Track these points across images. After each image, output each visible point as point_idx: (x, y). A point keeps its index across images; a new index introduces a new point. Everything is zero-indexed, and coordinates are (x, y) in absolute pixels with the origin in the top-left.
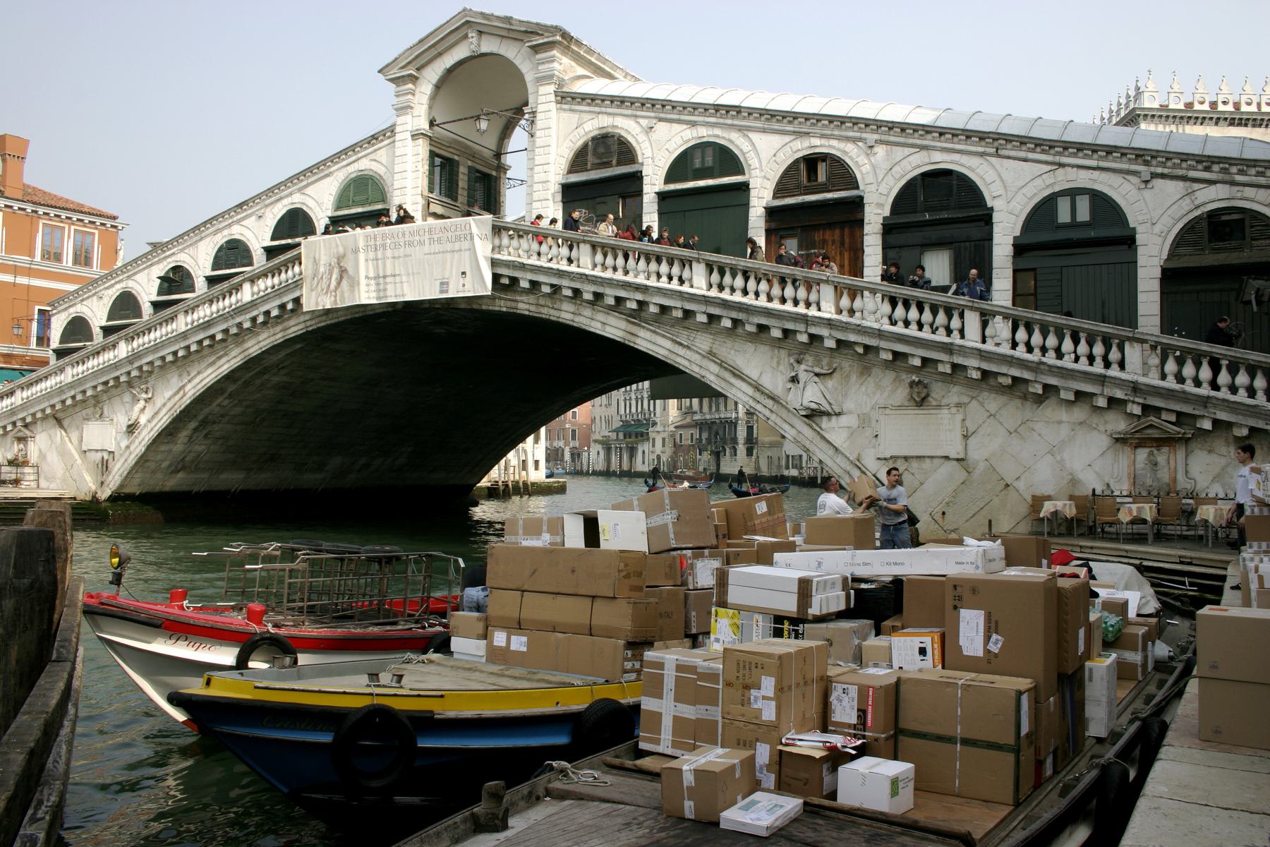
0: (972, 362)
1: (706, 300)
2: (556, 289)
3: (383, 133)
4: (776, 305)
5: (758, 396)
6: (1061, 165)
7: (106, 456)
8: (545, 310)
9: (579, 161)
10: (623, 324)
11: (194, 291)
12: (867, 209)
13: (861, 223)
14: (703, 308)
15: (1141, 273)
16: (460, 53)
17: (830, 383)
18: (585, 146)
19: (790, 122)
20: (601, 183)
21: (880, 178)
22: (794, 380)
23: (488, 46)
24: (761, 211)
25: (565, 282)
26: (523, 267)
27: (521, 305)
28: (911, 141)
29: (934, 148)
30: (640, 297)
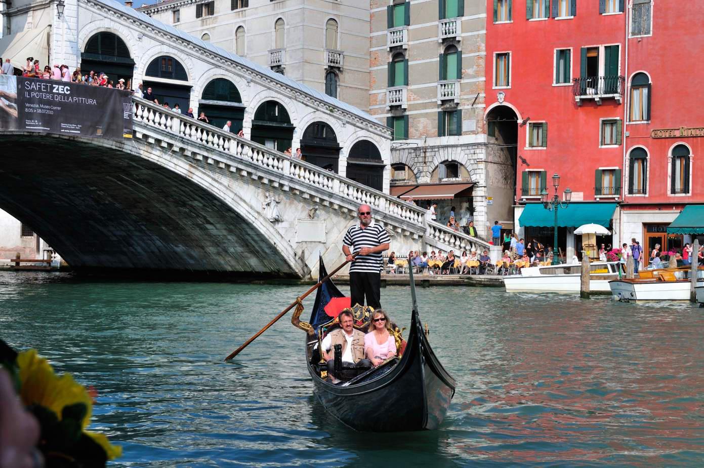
2: (158, 141)
5: (250, 210)
6: (318, 110)
8: (142, 152)
10: (187, 167)
12: (245, 115)
14: (235, 164)
17: (279, 205)
19: (213, 58)
21: (252, 98)
22: (268, 205)
25: (167, 140)
27: (126, 147)
28: (264, 84)
29: (273, 90)
30: (206, 154)
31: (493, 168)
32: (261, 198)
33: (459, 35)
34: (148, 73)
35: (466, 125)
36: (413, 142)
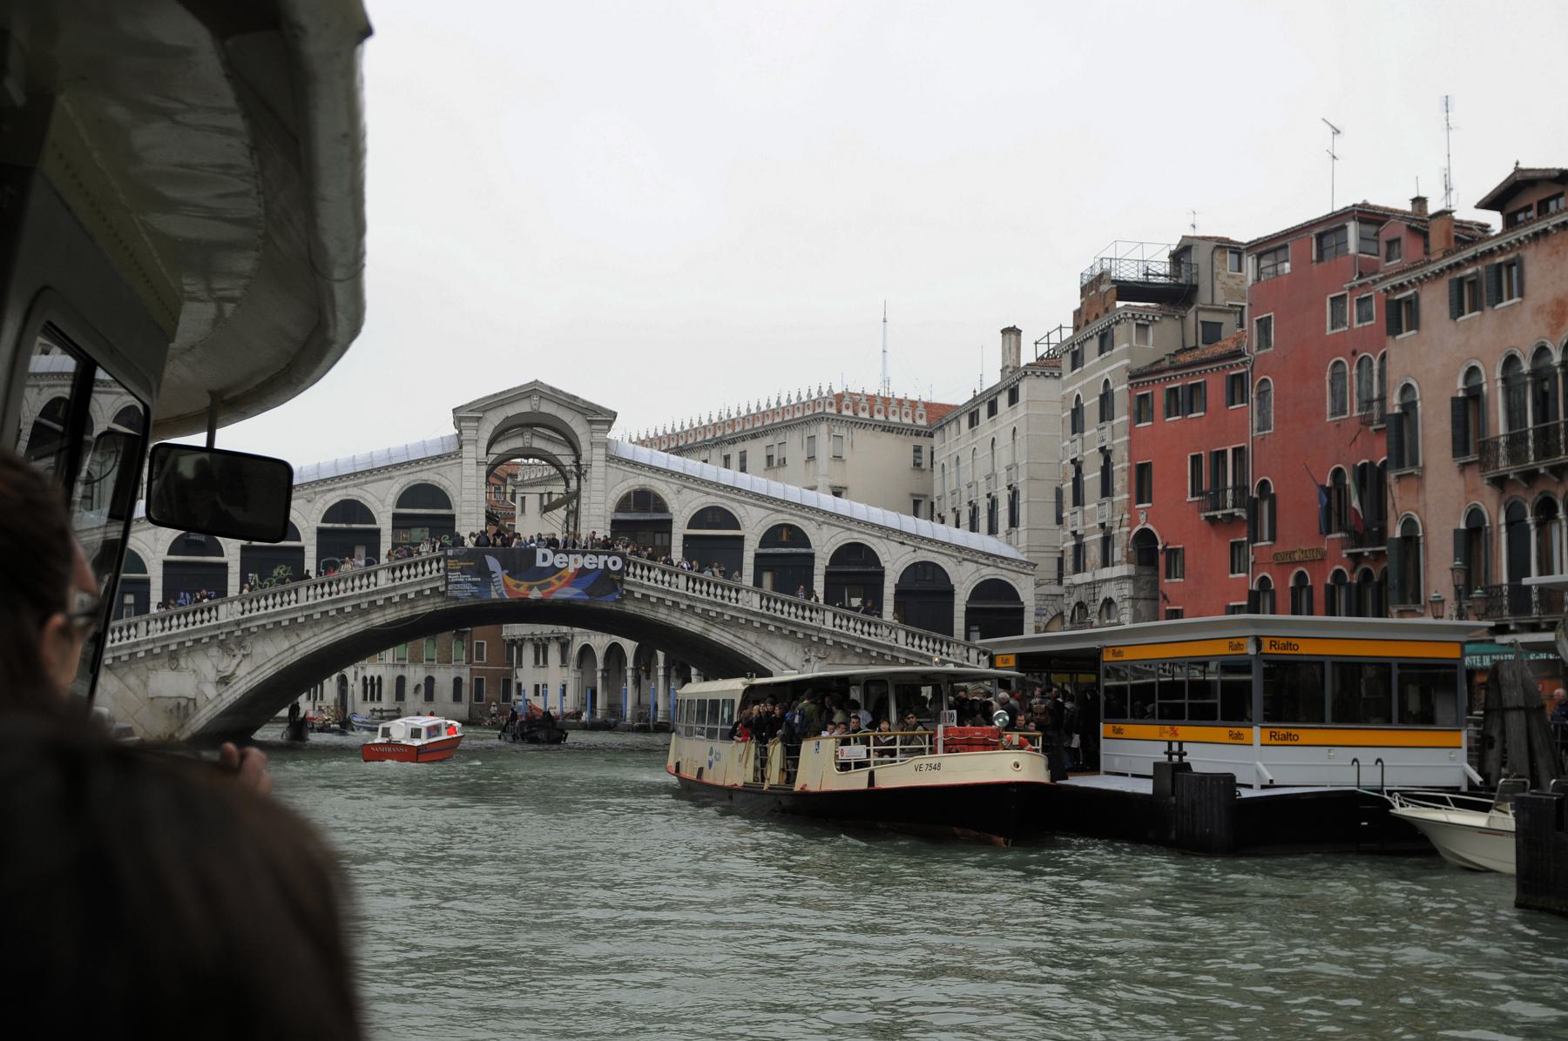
0: (902, 655)
1: (763, 615)
3: (449, 455)
4: (800, 620)
7: (183, 702)
9: (623, 505)
11: (222, 555)
13: (812, 567)
15: (956, 608)
16: (524, 407)
18: (628, 494)
20: (641, 520)
21: (824, 544)
23: (547, 408)
24: (752, 554)
26: (642, 586)
31: (1141, 605)
32: (800, 654)
33: (1107, 443)
35: (1118, 553)
36: (1087, 577)
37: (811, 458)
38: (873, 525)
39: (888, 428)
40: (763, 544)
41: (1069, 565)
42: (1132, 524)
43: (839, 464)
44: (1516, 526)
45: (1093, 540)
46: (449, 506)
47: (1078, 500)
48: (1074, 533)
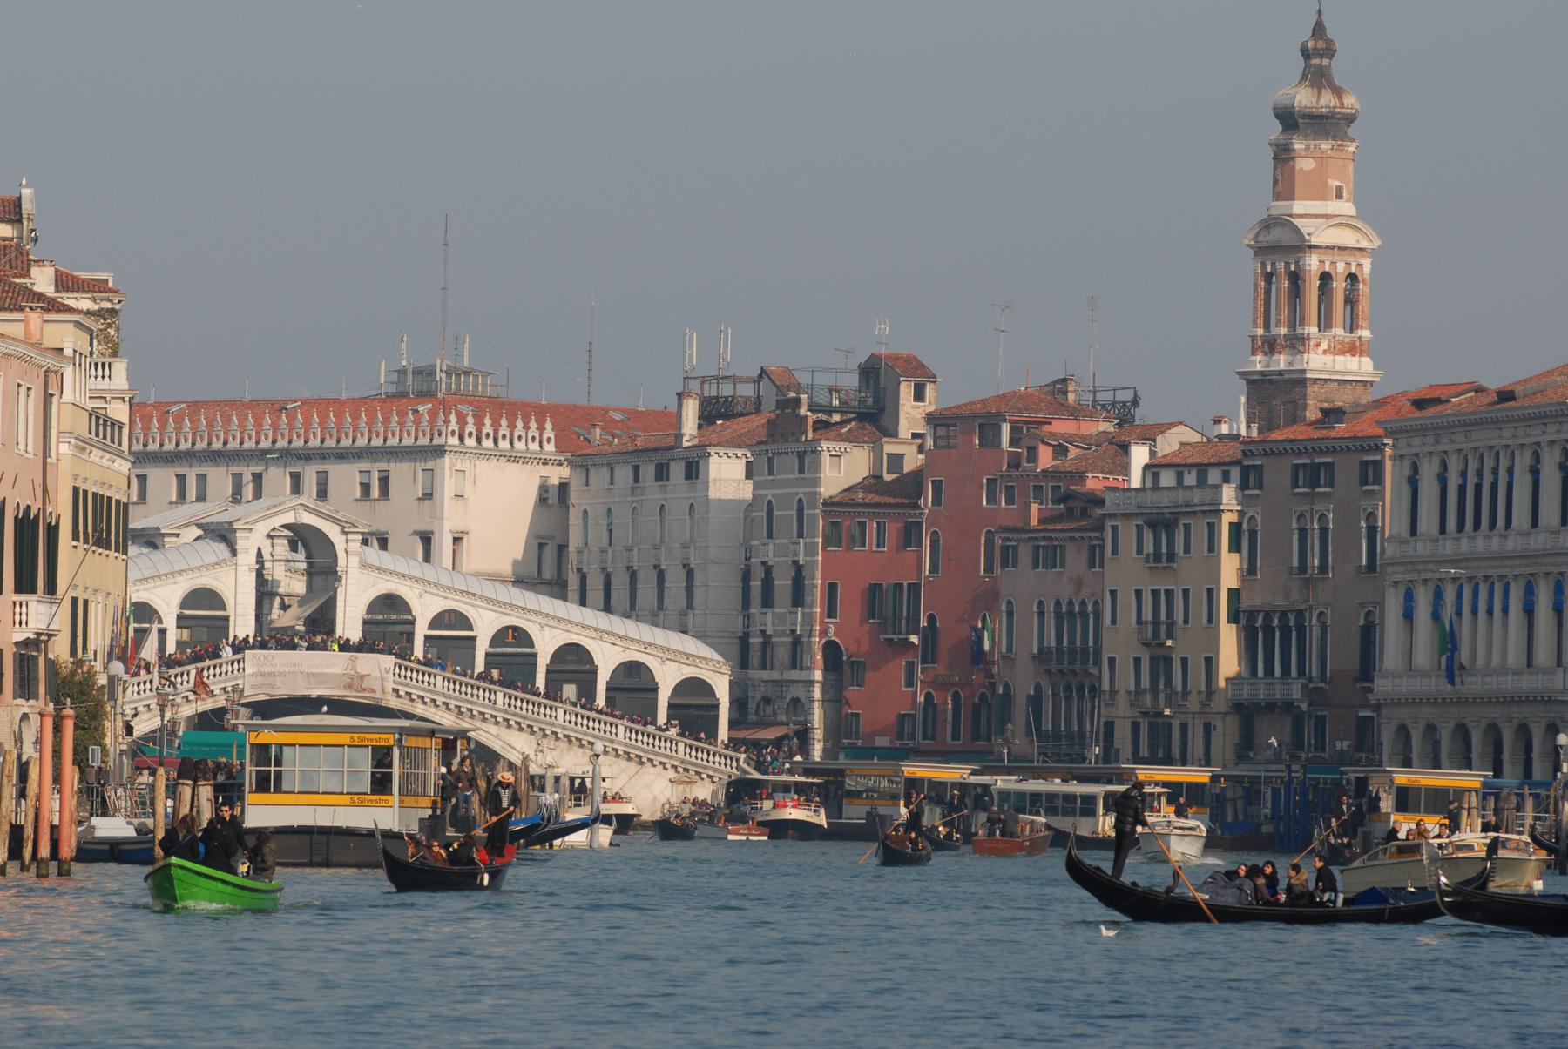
9: (372, 608)
20: (387, 625)
21: (546, 644)
34: (430, 628)
36: (775, 675)
37: (428, 495)
38: (589, 628)
39: (515, 460)
40: (491, 645)
41: (755, 659)
42: (824, 633)
43: (461, 503)
44: (1055, 695)
45: (782, 643)
46: (224, 609)
47: (767, 601)
48: (763, 632)
